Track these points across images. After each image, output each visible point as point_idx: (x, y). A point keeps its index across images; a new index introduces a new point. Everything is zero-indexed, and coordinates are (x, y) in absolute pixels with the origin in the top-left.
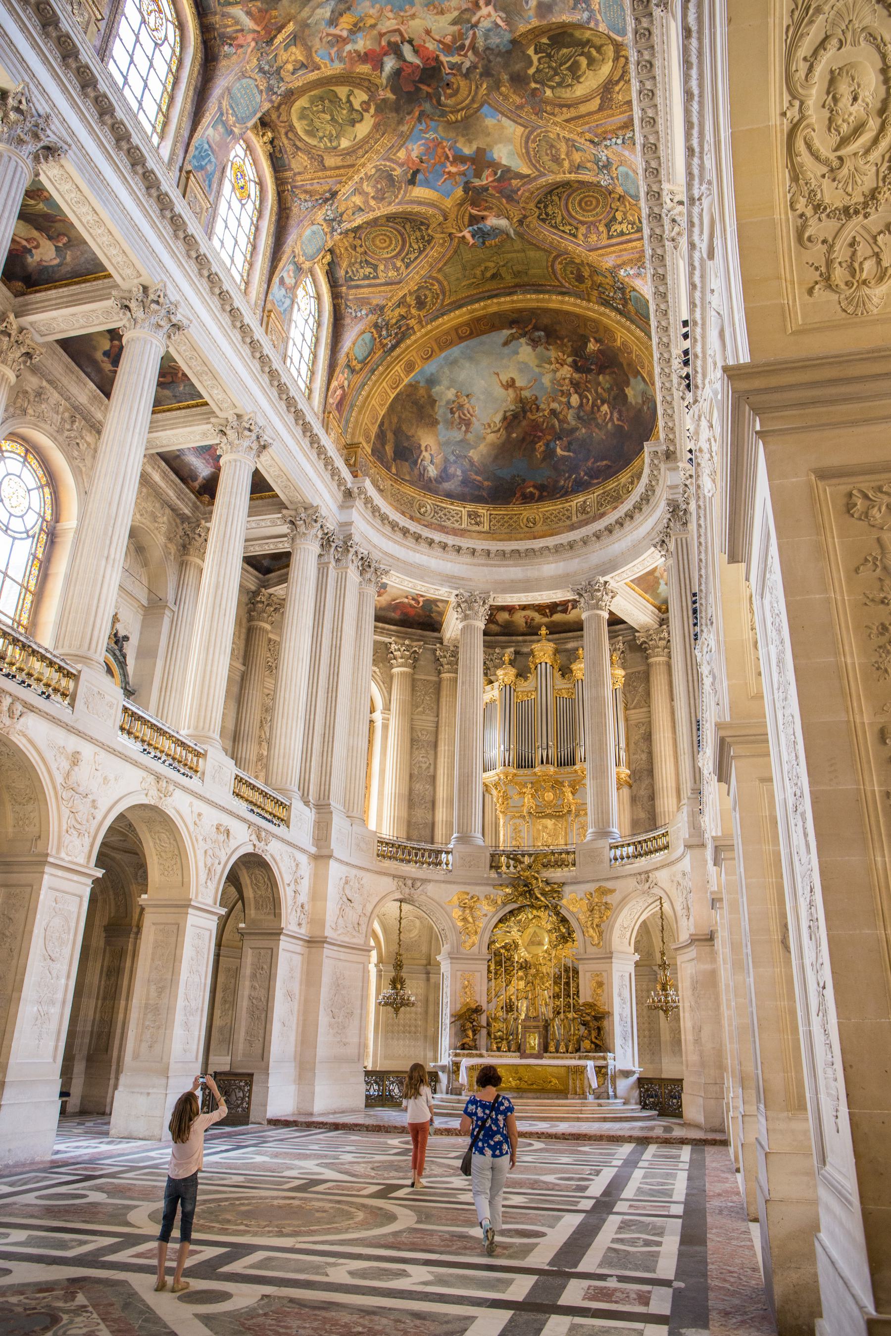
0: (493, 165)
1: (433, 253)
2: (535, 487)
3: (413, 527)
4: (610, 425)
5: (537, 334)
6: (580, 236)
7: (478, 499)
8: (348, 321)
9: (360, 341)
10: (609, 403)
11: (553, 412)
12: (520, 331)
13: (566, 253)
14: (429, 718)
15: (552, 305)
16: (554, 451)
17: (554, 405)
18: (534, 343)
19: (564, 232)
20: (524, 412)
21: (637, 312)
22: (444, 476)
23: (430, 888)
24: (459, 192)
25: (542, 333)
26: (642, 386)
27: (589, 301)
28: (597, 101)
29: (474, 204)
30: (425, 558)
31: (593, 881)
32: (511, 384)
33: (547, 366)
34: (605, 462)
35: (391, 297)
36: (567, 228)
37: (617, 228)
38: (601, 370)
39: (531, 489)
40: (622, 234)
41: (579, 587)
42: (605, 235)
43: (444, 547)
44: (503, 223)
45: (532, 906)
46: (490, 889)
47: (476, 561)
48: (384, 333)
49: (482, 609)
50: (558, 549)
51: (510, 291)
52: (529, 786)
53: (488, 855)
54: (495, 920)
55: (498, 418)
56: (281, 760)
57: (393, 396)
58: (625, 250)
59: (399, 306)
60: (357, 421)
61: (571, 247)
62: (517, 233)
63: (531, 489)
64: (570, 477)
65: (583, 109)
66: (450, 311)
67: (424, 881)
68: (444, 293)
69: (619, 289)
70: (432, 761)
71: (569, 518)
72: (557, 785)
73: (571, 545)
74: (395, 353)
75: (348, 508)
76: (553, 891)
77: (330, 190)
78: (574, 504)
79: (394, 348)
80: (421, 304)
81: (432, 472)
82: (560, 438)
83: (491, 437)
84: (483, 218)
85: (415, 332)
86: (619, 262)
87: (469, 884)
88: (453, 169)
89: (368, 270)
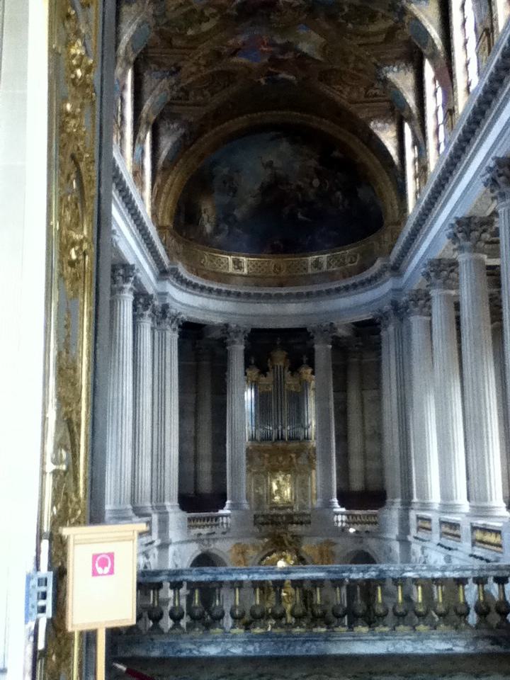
0: (297, 51)
1: (234, 89)
4: (341, 208)
7: (238, 251)
8: (162, 130)
11: (299, 188)
17: (300, 183)
22: (217, 230)
24: (266, 60)
28: (384, 36)
29: (273, 67)
32: (270, 165)
37: (372, 91)
39: (278, 242)
40: (376, 95)
41: (313, 326)
43: (219, 292)
44: (291, 77)
47: (239, 299)
48: (188, 138)
49: (243, 336)
53: (252, 516)
54: (257, 561)
55: (257, 187)
60: (164, 207)
61: (337, 98)
63: (278, 242)
65: (372, 40)
67: (214, 540)
71: (305, 269)
72: (285, 452)
73: (309, 295)
74: (191, 149)
77: (175, 65)
79: (191, 145)
81: (208, 228)
83: (251, 201)
84: (277, 74)
85: (206, 132)
86: (371, 114)
88: (265, 49)
89: (181, 94)
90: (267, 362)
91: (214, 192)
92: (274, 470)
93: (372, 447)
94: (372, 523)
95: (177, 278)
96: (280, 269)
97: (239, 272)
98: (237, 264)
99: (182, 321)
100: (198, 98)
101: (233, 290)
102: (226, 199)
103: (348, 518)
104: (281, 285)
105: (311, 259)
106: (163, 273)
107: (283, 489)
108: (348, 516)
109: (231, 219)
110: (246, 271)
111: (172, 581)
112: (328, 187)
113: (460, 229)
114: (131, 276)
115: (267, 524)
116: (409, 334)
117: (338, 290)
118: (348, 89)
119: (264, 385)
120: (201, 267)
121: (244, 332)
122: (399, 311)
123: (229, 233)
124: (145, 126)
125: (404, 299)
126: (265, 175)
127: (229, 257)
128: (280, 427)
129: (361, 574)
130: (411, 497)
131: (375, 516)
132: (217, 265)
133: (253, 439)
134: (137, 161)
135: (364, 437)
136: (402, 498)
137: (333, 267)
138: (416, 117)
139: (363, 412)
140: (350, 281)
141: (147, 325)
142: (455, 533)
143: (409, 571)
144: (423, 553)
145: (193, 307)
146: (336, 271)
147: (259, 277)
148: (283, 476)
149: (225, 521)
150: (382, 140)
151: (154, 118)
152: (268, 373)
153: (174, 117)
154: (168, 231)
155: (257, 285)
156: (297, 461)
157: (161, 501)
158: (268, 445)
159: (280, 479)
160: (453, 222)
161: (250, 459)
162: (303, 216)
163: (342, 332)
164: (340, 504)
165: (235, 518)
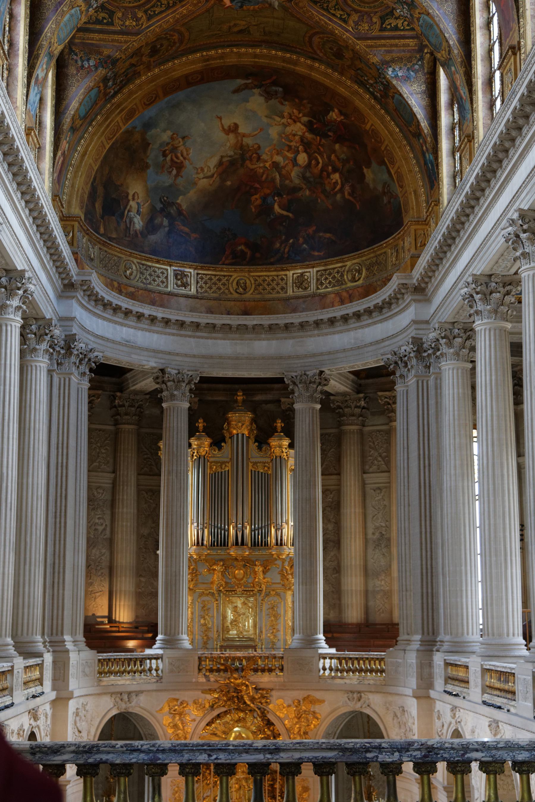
2: (247, 245)
3: (125, 303)
4: (339, 196)
5: (274, 88)
6: (351, 22)
8: (72, 70)
9: (87, 99)
10: (341, 174)
11: (275, 165)
12: (256, 83)
13: (332, 33)
14: (105, 474)
15: (300, 69)
16: (273, 208)
17: (278, 159)
18: (268, 95)
19: (334, 15)
20: (243, 158)
21: (396, 110)
22: (151, 227)
23: (142, 698)
25: (281, 89)
26: (385, 176)
27: (342, 74)
30: (132, 331)
31: (302, 689)
32: (234, 129)
33: (278, 119)
34: (328, 235)
35: (125, 50)
36: (338, 13)
38: (339, 139)
39: (242, 247)
40: (396, 28)
41: (294, 374)
42: (377, 26)
43: (153, 319)
45: (238, 709)
46: (198, 694)
47: (182, 332)
49: (188, 388)
50: (272, 328)
51: (254, 45)
52: (222, 563)
53: (197, 658)
54: (204, 724)
55: (213, 162)
56: (26, 610)
57: (108, 147)
58: (396, 45)
59: (132, 57)
60: (73, 186)
61: (338, 31)
62: (279, 3)
63: (242, 247)
64: (287, 240)
66: (182, 55)
67: (138, 693)
68: (181, 42)
69: (382, 83)
70: (108, 522)
72: (248, 563)
73: (287, 327)
75: (68, 298)
76: (263, 697)
78: (292, 272)
80: (154, 51)
81: (138, 223)
82: (279, 195)
83: (203, 183)
86: (388, 58)
87: (179, 690)
89: (102, 15)
90: (223, 429)
91: (147, 166)
92: (229, 590)
93: (376, 558)
94: (377, 671)
95: (89, 296)
96: (245, 289)
97: (182, 291)
98: (180, 276)
99: (94, 362)
100: (127, 23)
101: (173, 317)
102: (166, 180)
103: (341, 664)
104: (246, 313)
105: (292, 274)
106: (67, 287)
107: (241, 618)
108: (339, 659)
109: (173, 211)
110: (193, 291)
111: (81, 762)
112: (320, 165)
113: (525, 227)
114: (19, 289)
115: (218, 670)
116: (438, 387)
117: (332, 321)
118: (355, 17)
119: (216, 462)
120: (125, 280)
121: (189, 383)
122: (423, 353)
123: (169, 232)
124: (46, 59)
125: (432, 335)
126: (226, 145)
127: (168, 268)
128: (240, 526)
129: (397, 754)
130: (435, 632)
131: (381, 660)
132: (150, 279)
133: (199, 543)
134: (32, 113)
135: (366, 541)
136: (423, 634)
137: (326, 287)
138: (459, 60)
139: (364, 507)
140: (350, 309)
141: (41, 363)
142: (507, 687)
143: (477, 750)
144: (454, 716)
145: (113, 342)
146: (329, 293)
147: (215, 299)
148: (243, 599)
149: (154, 666)
150: (405, 96)
151: (60, 48)
152: (223, 444)
153: (91, 50)
154: (76, 224)
155: (210, 311)
156: (264, 578)
157: (57, 635)
158: (221, 552)
159: (239, 603)
160: (516, 216)
161: (194, 573)
162: (280, 208)
163: (336, 385)
164: (327, 641)
165: (171, 664)
